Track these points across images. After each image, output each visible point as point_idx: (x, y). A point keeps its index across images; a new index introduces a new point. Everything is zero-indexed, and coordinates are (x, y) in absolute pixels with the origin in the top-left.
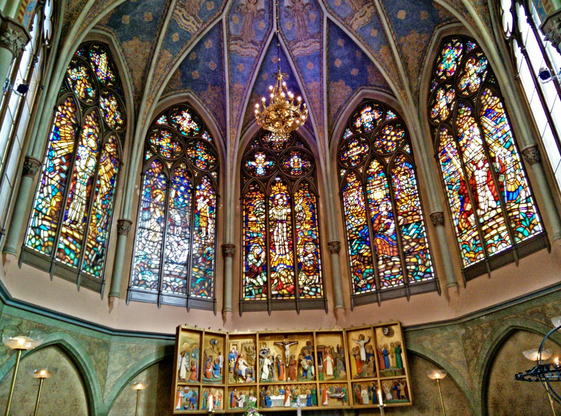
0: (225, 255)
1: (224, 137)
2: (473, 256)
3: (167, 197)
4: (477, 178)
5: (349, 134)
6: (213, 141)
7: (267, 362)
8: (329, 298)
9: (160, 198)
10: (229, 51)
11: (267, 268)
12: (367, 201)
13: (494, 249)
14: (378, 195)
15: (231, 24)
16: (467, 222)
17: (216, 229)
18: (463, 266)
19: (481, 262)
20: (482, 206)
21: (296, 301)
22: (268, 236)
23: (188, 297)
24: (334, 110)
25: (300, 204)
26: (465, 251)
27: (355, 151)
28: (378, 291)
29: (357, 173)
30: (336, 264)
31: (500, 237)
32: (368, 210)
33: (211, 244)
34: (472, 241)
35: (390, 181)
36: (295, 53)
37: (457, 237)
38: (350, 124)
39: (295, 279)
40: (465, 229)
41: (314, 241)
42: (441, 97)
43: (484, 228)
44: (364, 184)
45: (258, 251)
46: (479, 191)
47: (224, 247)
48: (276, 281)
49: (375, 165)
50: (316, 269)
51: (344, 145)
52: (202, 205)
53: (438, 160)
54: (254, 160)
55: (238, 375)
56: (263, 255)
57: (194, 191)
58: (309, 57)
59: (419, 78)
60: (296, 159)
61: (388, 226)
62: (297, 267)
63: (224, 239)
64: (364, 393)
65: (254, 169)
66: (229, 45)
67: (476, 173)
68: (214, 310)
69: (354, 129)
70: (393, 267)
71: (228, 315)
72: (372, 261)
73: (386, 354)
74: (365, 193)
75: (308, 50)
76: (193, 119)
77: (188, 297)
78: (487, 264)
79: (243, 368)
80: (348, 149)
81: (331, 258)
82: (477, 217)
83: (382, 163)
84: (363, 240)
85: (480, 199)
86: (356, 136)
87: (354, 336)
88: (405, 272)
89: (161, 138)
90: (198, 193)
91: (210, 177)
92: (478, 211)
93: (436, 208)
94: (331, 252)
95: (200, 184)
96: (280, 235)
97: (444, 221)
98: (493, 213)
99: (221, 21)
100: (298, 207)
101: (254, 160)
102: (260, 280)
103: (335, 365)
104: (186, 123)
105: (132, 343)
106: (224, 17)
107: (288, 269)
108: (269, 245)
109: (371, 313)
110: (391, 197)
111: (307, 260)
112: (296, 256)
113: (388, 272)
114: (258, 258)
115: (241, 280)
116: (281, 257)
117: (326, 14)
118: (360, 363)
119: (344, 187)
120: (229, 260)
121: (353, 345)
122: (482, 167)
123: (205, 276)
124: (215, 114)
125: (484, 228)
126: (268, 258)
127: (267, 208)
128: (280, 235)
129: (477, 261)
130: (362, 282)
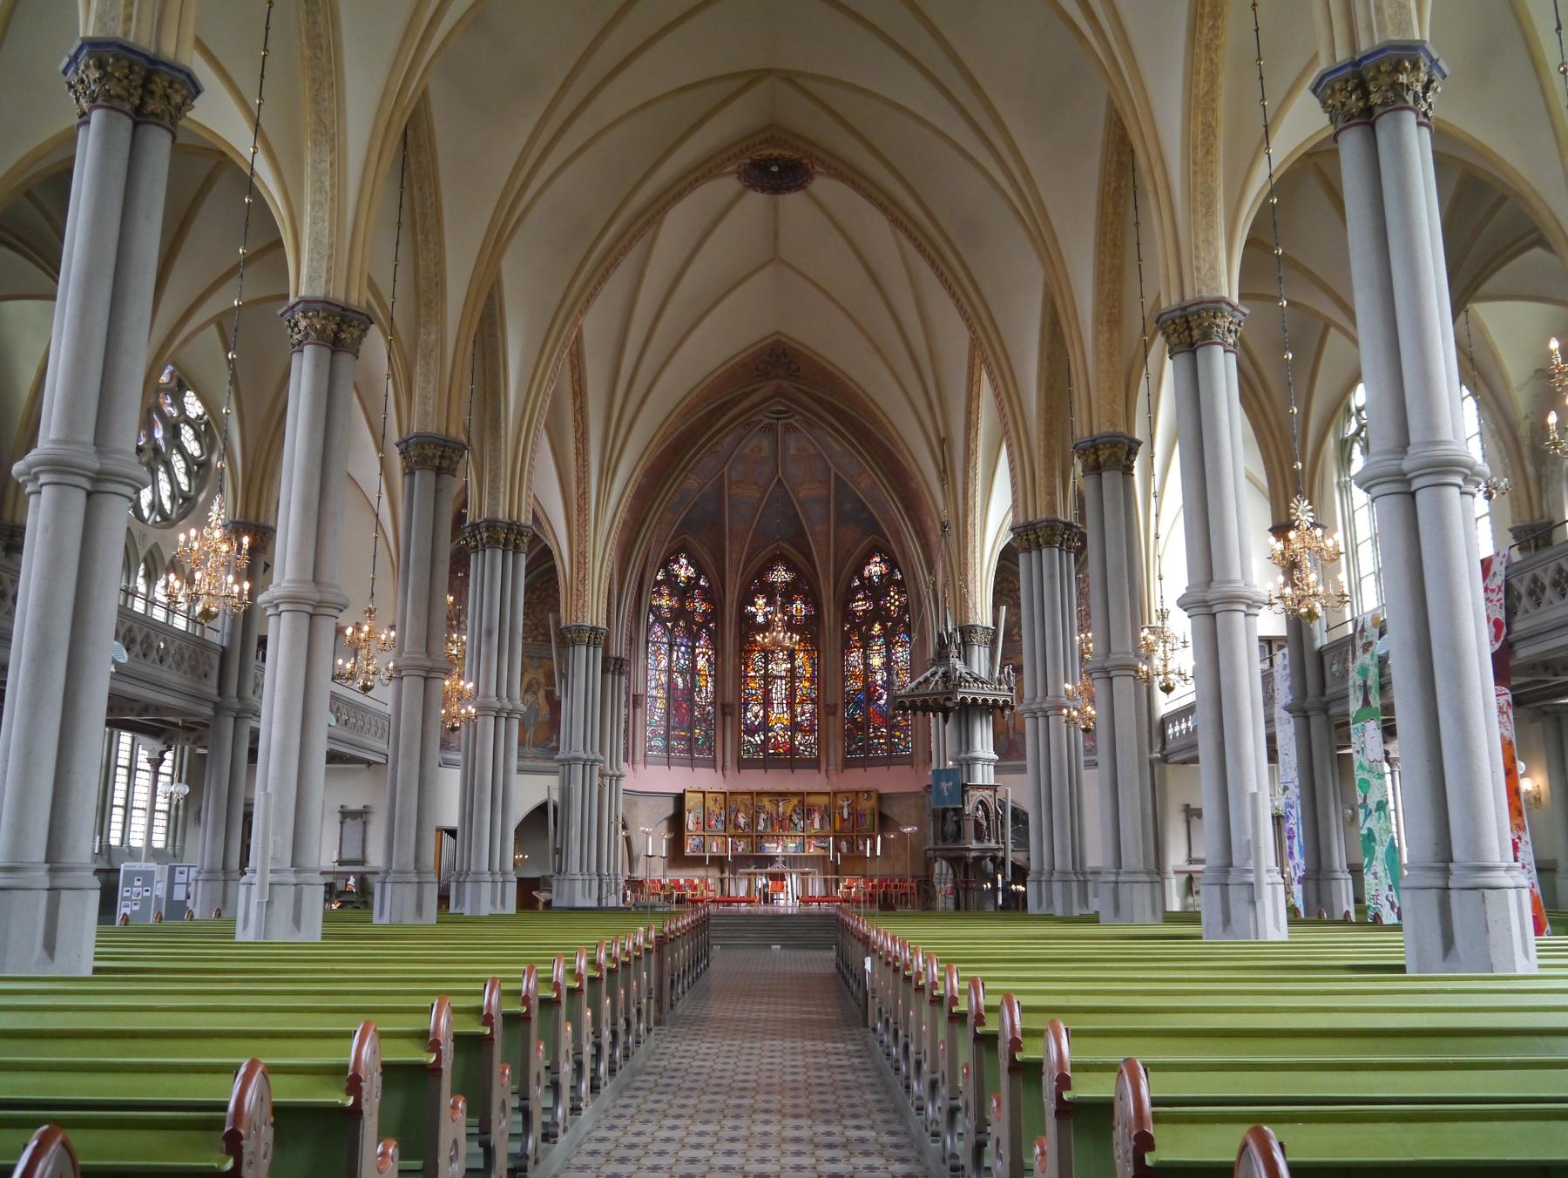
0: (724, 714)
1: (723, 579)
3: (670, 661)
5: (857, 583)
7: (763, 816)
8: (823, 758)
9: (664, 663)
11: (765, 726)
12: (867, 666)
14: (876, 661)
21: (789, 760)
23: (692, 758)
25: (801, 658)
27: (860, 606)
29: (860, 631)
30: (831, 728)
32: (866, 677)
35: (888, 650)
36: (801, 495)
39: (792, 738)
45: (756, 708)
47: (723, 706)
49: (877, 627)
50: (812, 731)
51: (850, 595)
52: (701, 663)
54: (754, 604)
55: (737, 826)
57: (693, 648)
60: (798, 605)
61: (880, 697)
62: (794, 727)
65: (755, 615)
69: (862, 577)
70: (881, 737)
71: (728, 772)
72: (862, 727)
74: (866, 657)
76: (689, 563)
77: (692, 758)
79: (742, 821)
83: (883, 626)
84: (858, 705)
86: (862, 587)
89: (661, 595)
94: (828, 714)
96: (779, 691)
100: (798, 662)
101: (754, 604)
102: (758, 739)
103: (822, 820)
104: (684, 571)
105: (653, 801)
107: (785, 729)
108: (767, 703)
109: (859, 779)
110: (888, 666)
112: (793, 716)
114: (756, 716)
117: (833, 469)
118: (843, 820)
120: (729, 719)
126: (766, 716)
127: (766, 663)
128: (779, 691)
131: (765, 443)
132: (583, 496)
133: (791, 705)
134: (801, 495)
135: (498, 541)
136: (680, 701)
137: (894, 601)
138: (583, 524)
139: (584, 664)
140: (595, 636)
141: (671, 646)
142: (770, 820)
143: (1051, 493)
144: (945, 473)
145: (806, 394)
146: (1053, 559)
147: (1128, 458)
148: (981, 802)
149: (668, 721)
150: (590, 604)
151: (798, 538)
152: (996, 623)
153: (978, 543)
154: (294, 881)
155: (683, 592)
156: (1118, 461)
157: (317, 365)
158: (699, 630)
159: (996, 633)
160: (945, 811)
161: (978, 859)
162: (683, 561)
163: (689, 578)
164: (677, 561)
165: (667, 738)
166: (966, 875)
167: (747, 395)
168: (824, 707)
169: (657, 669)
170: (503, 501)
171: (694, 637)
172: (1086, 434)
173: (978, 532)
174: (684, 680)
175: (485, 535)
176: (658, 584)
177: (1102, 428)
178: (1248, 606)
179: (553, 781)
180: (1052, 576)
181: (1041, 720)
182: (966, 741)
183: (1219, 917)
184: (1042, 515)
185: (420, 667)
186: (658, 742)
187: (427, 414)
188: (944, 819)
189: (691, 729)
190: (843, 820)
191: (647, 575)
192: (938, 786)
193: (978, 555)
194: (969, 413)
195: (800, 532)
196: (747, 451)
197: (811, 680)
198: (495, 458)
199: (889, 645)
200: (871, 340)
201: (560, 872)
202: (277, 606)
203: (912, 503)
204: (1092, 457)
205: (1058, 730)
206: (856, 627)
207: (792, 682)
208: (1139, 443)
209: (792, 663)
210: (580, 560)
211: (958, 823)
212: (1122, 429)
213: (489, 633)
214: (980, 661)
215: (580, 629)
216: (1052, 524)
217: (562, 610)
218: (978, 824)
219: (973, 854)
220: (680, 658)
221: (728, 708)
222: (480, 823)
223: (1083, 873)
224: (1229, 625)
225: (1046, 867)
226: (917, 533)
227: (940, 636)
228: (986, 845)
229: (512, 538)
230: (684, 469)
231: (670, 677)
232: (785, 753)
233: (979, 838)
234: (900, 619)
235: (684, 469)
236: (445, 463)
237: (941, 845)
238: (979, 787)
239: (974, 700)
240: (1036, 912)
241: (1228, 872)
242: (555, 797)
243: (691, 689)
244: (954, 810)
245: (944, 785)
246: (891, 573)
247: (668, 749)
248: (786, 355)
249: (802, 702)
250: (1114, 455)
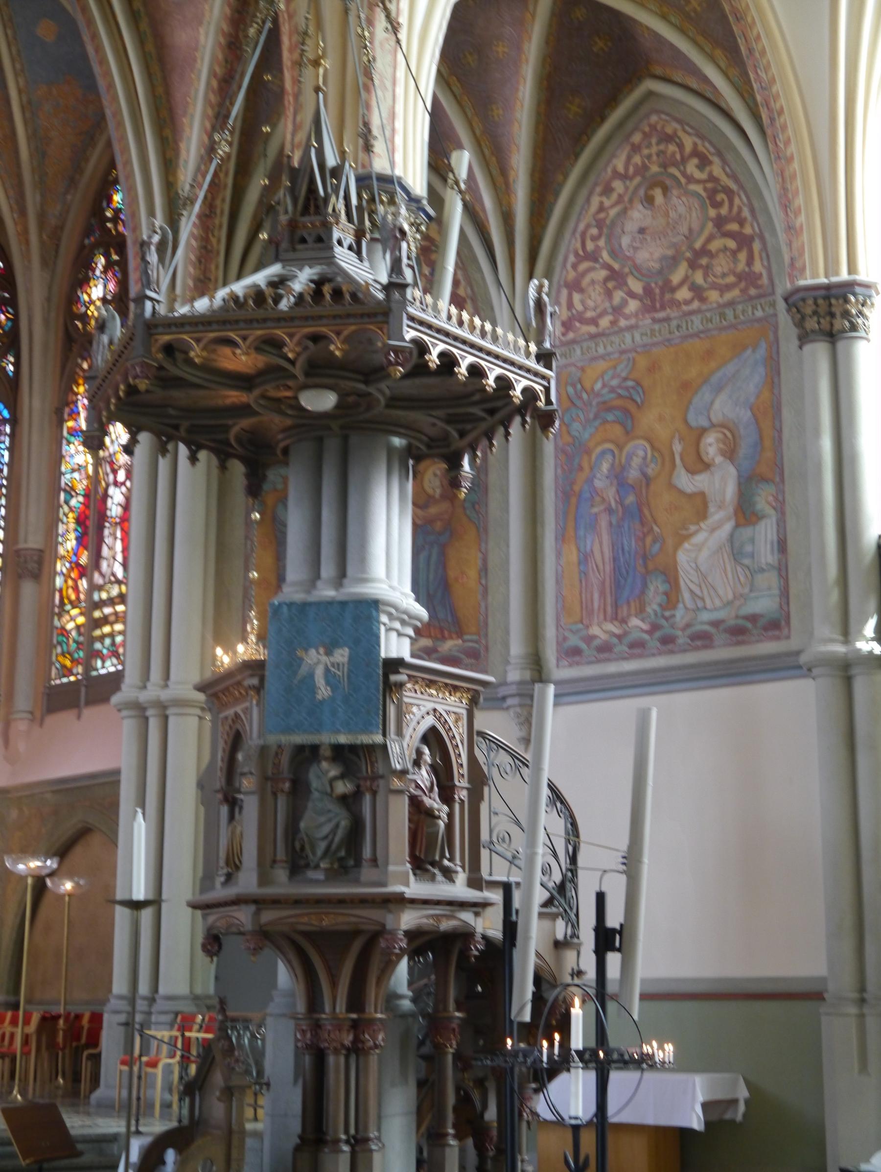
2: (68, 663)
4: (109, 501)
13: (99, 663)
16: (76, 589)
18: (50, 679)
19: (78, 681)
20: (104, 565)
26: (59, 650)
31: (113, 643)
34: (74, 633)
37: (53, 614)
40: (71, 602)
42: (98, 273)
43: (97, 614)
46: (106, 532)
53: (61, 422)
59: (69, 197)
67: (112, 490)
78: (83, 690)
82: (94, 587)
85: (105, 551)
92: (96, 575)
93: (32, 541)
97: (40, 569)
98: (115, 591)
122: (123, 484)
125: (97, 614)
129: (72, 678)
160: (307, 754)
166: (356, 1002)
181: (154, 725)
188: (299, 789)
192: (293, 663)
218: (419, 812)
219: (408, 919)
225: (144, 989)
228: (441, 889)
233: (423, 862)
237: (282, 884)
244: (340, 753)
245: (317, 662)
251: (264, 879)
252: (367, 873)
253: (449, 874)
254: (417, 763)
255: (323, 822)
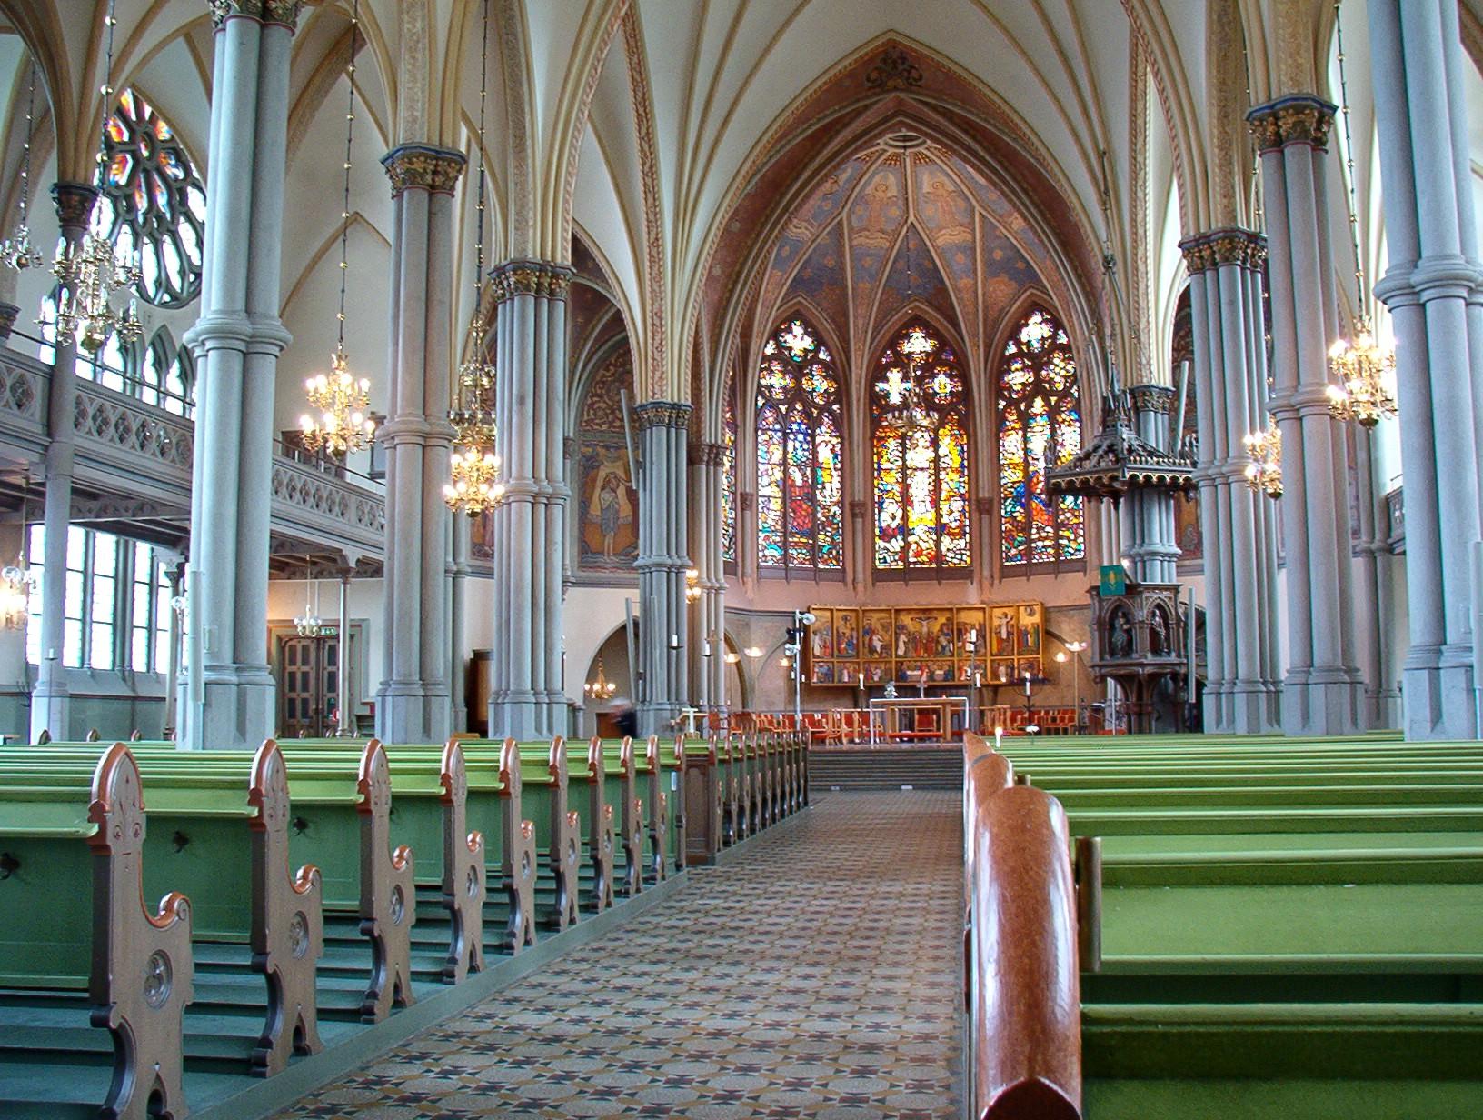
0: (854, 515)
1: (847, 352)
3: (785, 452)
5: (1012, 349)
6: (833, 360)
7: (903, 638)
10: (851, 247)
11: (904, 530)
15: (854, 218)
17: (841, 482)
22: (905, 488)
23: (817, 570)
24: (993, 314)
25: (946, 445)
27: (1018, 378)
28: (1030, 564)
32: (1027, 464)
33: (836, 503)
35: (1053, 431)
36: (940, 242)
38: (1014, 335)
39: (938, 543)
41: (962, 496)
44: (1026, 428)
47: (852, 505)
48: (914, 547)
49: (1038, 406)
51: (1004, 365)
52: (825, 455)
54: (886, 380)
56: (899, 514)
57: (813, 437)
58: (959, 248)
62: (940, 529)
63: (852, 494)
64: (1002, 669)
65: (887, 395)
66: (850, 240)
68: (844, 580)
69: (1018, 343)
71: (860, 586)
73: (1027, 633)
74: (1026, 440)
75: (957, 239)
76: (806, 333)
79: (877, 644)
80: (1009, 371)
81: (980, 520)
83: (1047, 403)
86: (1020, 355)
87: (998, 612)
88: (1057, 546)
90: (818, 439)
91: (832, 413)
95: (821, 424)
96: (920, 486)
99: (840, 223)
101: (886, 380)
102: (897, 544)
104: (798, 341)
106: (844, 215)
108: (906, 501)
111: (950, 520)
112: (939, 516)
113: (1040, 544)
114: (894, 518)
115: (874, 543)
116: (921, 517)
117: (978, 209)
118: (1000, 640)
119: (999, 426)
121: (996, 622)
123: (833, 544)
124: (833, 320)
126: (905, 517)
127: (904, 452)
128: (920, 486)
130: (1014, 551)
131: (892, 179)
132: (656, 242)
133: (935, 503)
134: (940, 242)
135: (528, 287)
136: (798, 500)
137: (1058, 371)
138: (658, 278)
139: (662, 446)
140: (674, 415)
141: (785, 436)
142: (914, 640)
143: (1229, 195)
144: (1107, 195)
145: (934, 108)
146: (1233, 278)
147: (1318, 129)
148: (1158, 606)
149: (785, 526)
150: (663, 376)
151: (939, 297)
152: (1176, 382)
153: (1151, 283)
154: (234, 679)
155: (798, 369)
156: (1305, 132)
157: (241, 44)
158: (820, 414)
159: (1177, 394)
161: (1154, 677)
162: (798, 329)
163: (806, 351)
164: (789, 330)
165: (785, 546)
167: (859, 113)
168: (981, 506)
169: (770, 461)
170: (534, 236)
171: (813, 424)
172: (1262, 98)
173: (1151, 268)
174: (804, 475)
175: (512, 280)
176: (766, 358)
177: (1283, 88)
178: (1471, 290)
179: (635, 594)
180: (1233, 303)
182: (1140, 531)
183: (1427, 712)
184: (1218, 224)
185: (415, 433)
186: (776, 553)
187: (415, 120)
188: (1112, 627)
189: (812, 534)
190: (1000, 640)
191: (753, 348)
193: (1151, 297)
194: (1133, 116)
195: (942, 290)
196: (869, 190)
197: (960, 471)
198: (521, 186)
199: (1053, 423)
200: (1013, 38)
201: (644, 701)
202: (203, 344)
203: (1068, 238)
204: (1271, 129)
205: (1243, 499)
206: (1012, 403)
207: (937, 474)
208: (1335, 109)
209: (936, 451)
210: (656, 322)
211: (1128, 632)
212: (1309, 89)
213: (522, 401)
214: (1156, 429)
215: (657, 406)
216: (1231, 235)
217: (636, 385)
218: (1154, 634)
219: (1149, 670)
220: (797, 447)
221: (858, 509)
222: (519, 632)
223: (1275, 683)
224: (1447, 315)
226: (1079, 277)
227: (1105, 399)
229: (546, 282)
230: (786, 209)
231: (785, 472)
232: (930, 562)
233: (1156, 650)
234: (1065, 394)
235: (786, 209)
236: (439, 180)
238: (1156, 587)
239: (1147, 478)
240: (1214, 731)
241: (1440, 652)
242: (637, 612)
243: (812, 488)
246: (1054, 336)
247: (786, 558)
248: (904, 60)
249: (949, 498)
250: (1299, 125)
251: (1102, 658)
252: (1135, 655)
253: (1169, 654)
254: (1154, 615)
255: (1120, 638)
